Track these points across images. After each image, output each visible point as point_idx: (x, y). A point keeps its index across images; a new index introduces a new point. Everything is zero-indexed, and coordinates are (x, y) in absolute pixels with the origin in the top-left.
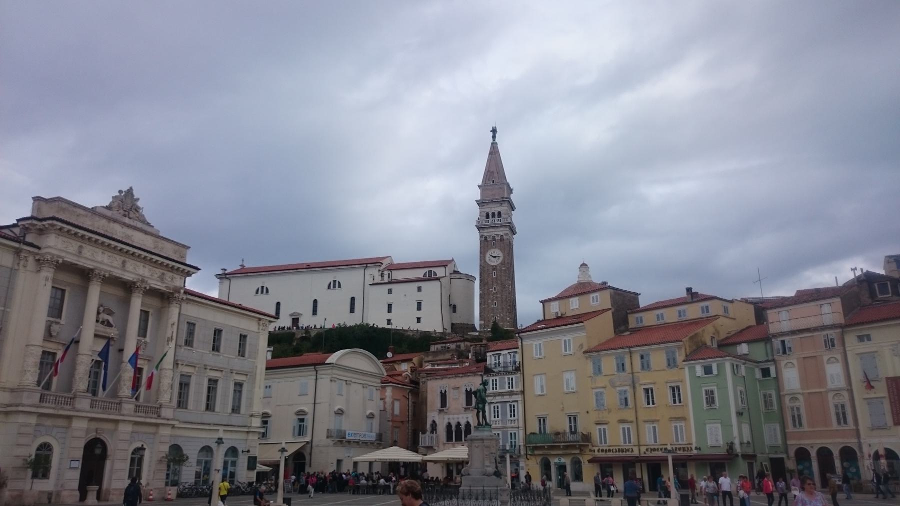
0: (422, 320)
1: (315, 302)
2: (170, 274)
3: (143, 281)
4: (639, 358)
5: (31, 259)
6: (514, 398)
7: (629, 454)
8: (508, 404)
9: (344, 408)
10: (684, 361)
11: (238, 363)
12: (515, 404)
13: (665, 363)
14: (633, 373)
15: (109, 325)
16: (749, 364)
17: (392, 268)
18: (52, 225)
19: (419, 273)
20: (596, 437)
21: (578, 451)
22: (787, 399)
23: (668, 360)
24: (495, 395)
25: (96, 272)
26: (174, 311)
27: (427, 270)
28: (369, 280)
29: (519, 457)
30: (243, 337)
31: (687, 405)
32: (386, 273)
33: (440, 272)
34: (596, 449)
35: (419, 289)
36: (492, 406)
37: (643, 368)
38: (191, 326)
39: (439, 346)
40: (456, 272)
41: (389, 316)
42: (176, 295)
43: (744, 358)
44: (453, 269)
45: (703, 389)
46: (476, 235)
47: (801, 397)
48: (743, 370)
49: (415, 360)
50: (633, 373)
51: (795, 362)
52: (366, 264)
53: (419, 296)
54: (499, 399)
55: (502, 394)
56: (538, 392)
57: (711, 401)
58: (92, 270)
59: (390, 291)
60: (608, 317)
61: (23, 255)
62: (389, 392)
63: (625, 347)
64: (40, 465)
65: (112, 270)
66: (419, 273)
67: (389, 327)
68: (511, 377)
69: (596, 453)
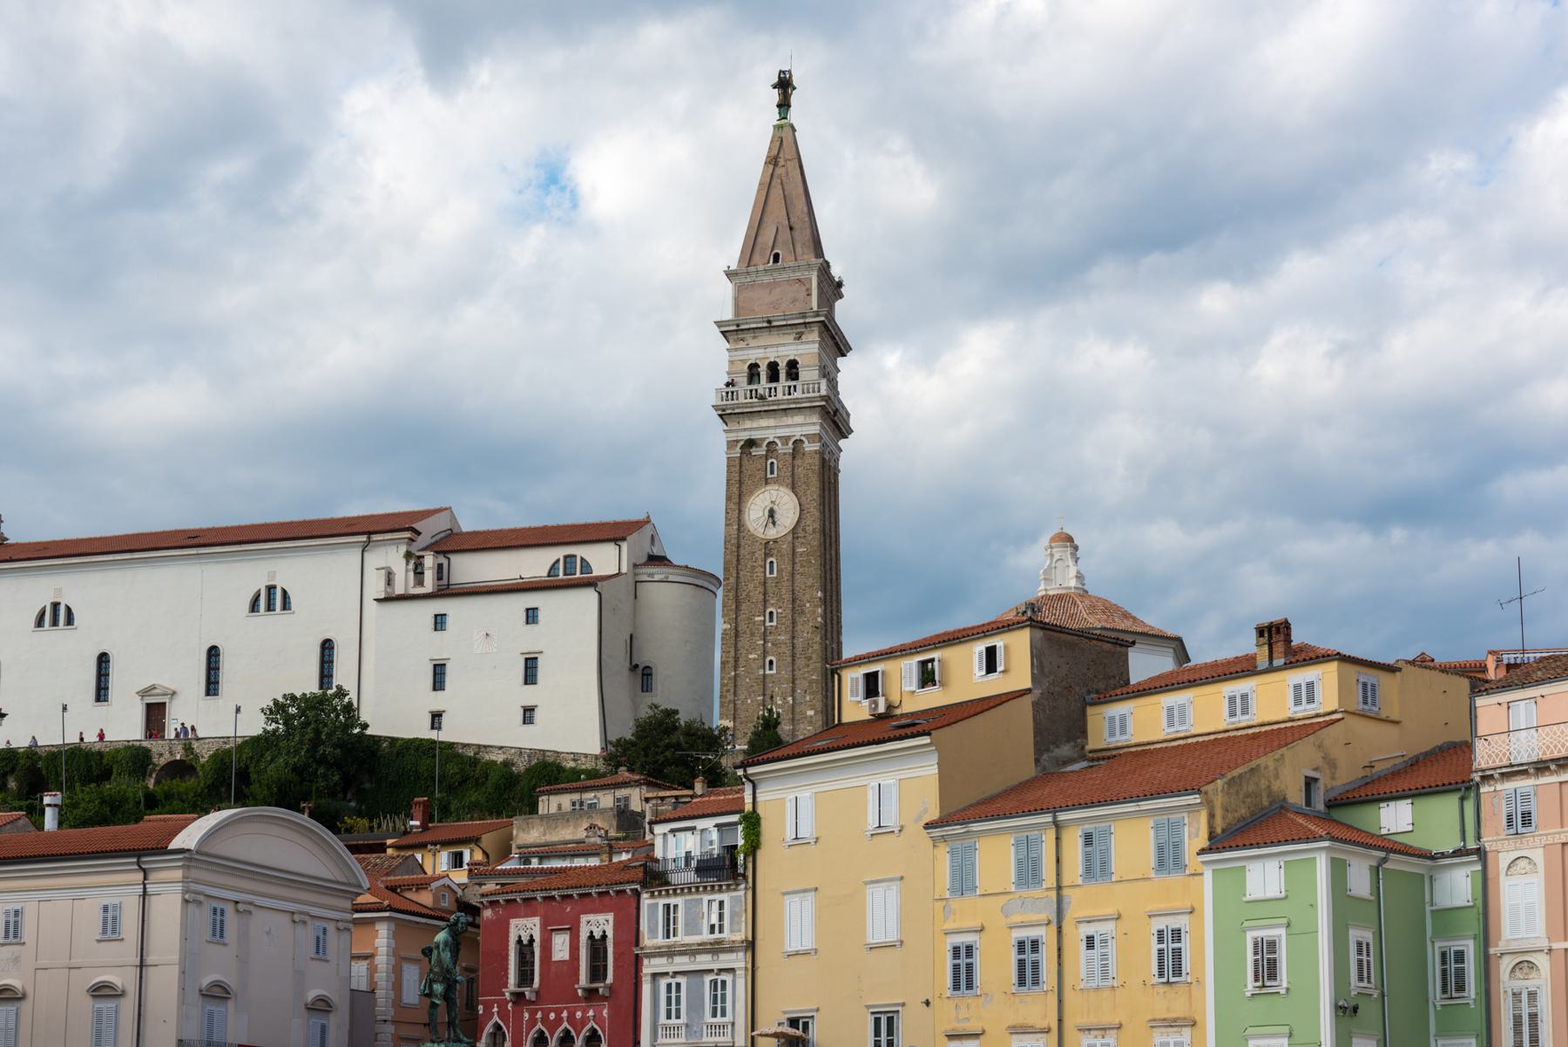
0: (538, 714)
4: (1080, 842)
6: (726, 960)
8: (708, 978)
10: (1202, 852)
12: (728, 978)
13: (1152, 861)
14: (1059, 888)
16: (1396, 863)
17: (453, 543)
19: (536, 563)
22: (1506, 965)
23: (1160, 849)
24: (670, 953)
27: (559, 553)
28: (375, 587)
32: (429, 561)
33: (603, 559)
35: (531, 616)
36: (663, 982)
37: (1089, 872)
39: (566, 801)
40: (657, 560)
43: (1390, 847)
44: (647, 549)
45: (1250, 936)
46: (714, 447)
47: (1542, 961)
48: (1360, 880)
49: (487, 840)
50: (1059, 888)
51: (1538, 855)
52: (367, 530)
53: (530, 640)
54: (682, 963)
55: (691, 951)
56: (795, 946)
59: (439, 622)
60: (1023, 715)
62: (382, 938)
63: (1042, 811)
67: (433, 735)
68: (718, 897)
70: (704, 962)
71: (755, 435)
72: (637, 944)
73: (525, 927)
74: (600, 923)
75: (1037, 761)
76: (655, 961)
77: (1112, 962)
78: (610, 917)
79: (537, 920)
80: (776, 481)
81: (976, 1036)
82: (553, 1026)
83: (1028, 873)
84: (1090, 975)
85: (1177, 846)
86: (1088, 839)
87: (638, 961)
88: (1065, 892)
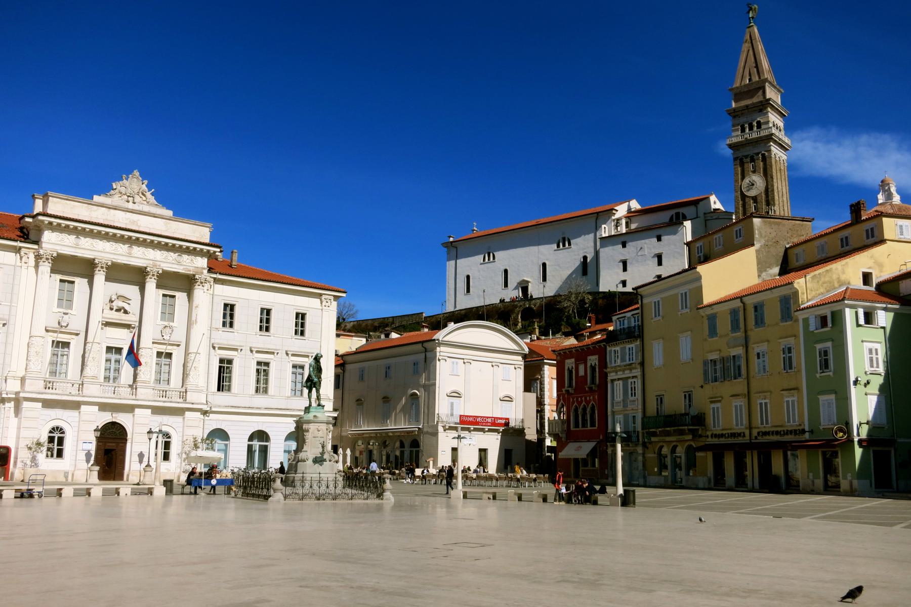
1: (544, 265)
2: (185, 257)
3: (155, 265)
4: (753, 310)
5: (32, 256)
7: (740, 440)
8: (630, 381)
9: (461, 390)
11: (298, 344)
13: (780, 317)
14: (746, 331)
15: (126, 312)
18: (43, 221)
19: (665, 217)
20: (710, 420)
21: (690, 437)
25: (96, 261)
26: (199, 292)
27: (673, 212)
29: (636, 445)
30: (301, 317)
31: (799, 371)
34: (709, 433)
35: (659, 239)
36: (615, 383)
37: (756, 323)
38: (229, 309)
41: (623, 276)
42: (197, 277)
50: (746, 331)
54: (620, 375)
57: (825, 365)
58: (94, 259)
61: (23, 251)
64: (56, 443)
65: (116, 257)
66: (665, 217)
68: (631, 346)
69: (710, 439)
70: (627, 374)
71: (746, 154)
72: (606, 367)
73: (570, 363)
74: (593, 360)
75: (759, 276)
76: (614, 374)
77: (767, 365)
78: (597, 357)
79: (573, 360)
80: (754, 172)
81: (719, 401)
82: (580, 403)
83: (735, 326)
84: (759, 370)
85: (788, 309)
86: (756, 308)
87: (606, 375)
88: (749, 333)
